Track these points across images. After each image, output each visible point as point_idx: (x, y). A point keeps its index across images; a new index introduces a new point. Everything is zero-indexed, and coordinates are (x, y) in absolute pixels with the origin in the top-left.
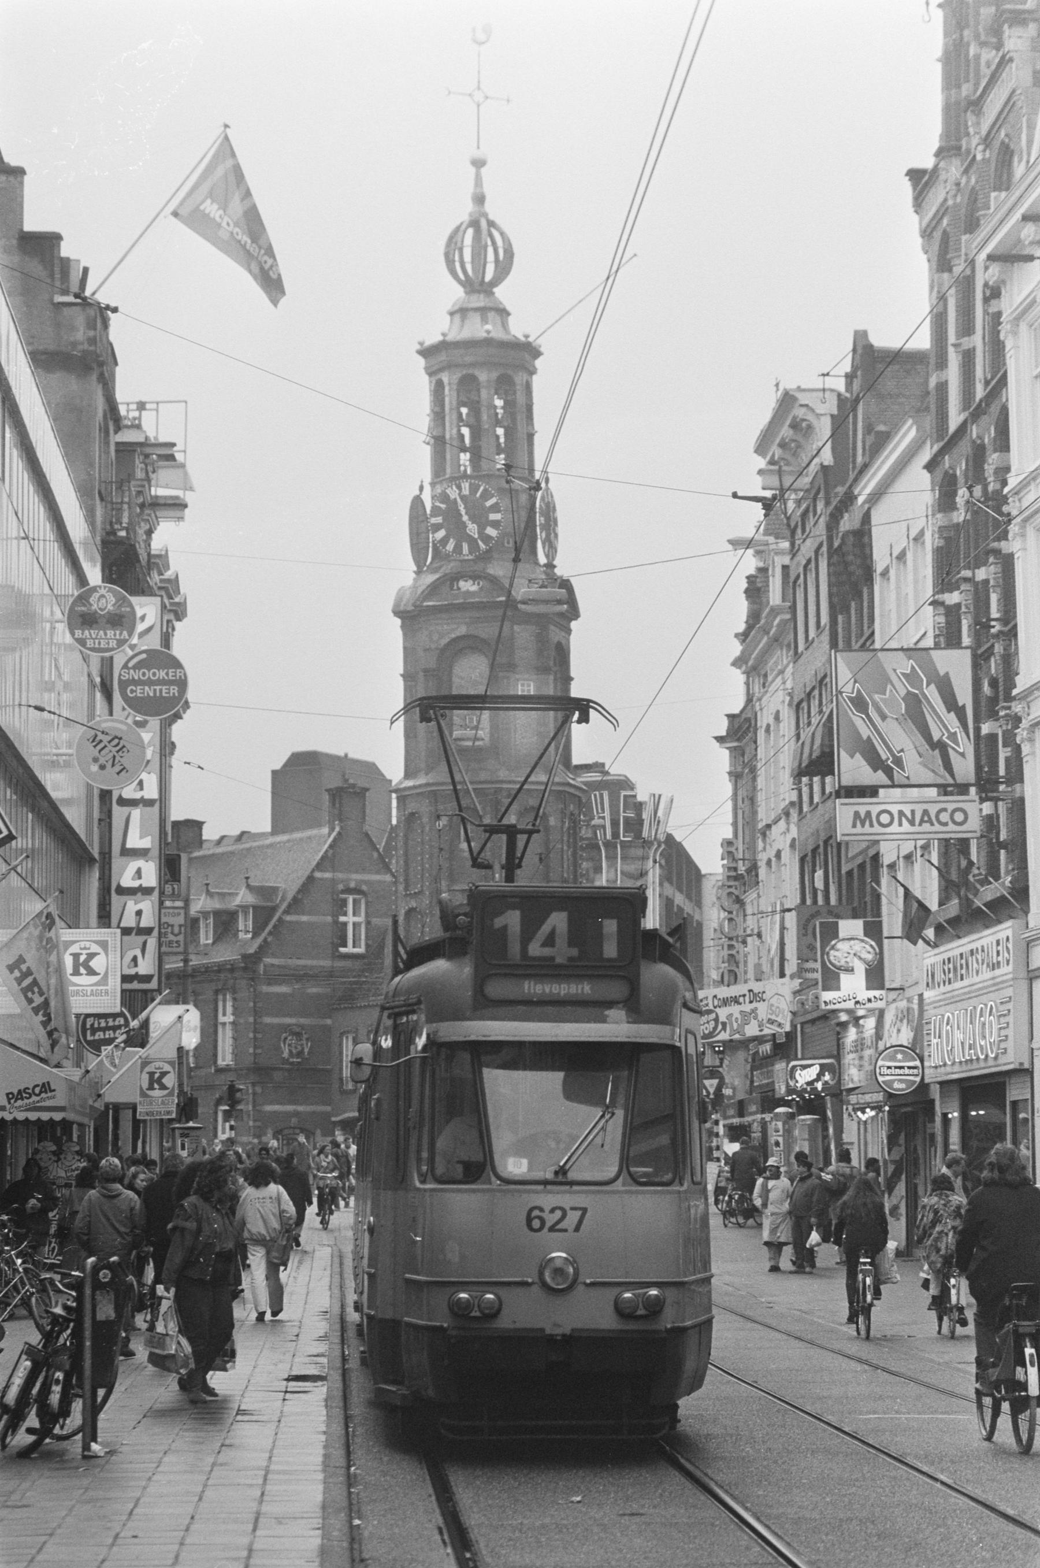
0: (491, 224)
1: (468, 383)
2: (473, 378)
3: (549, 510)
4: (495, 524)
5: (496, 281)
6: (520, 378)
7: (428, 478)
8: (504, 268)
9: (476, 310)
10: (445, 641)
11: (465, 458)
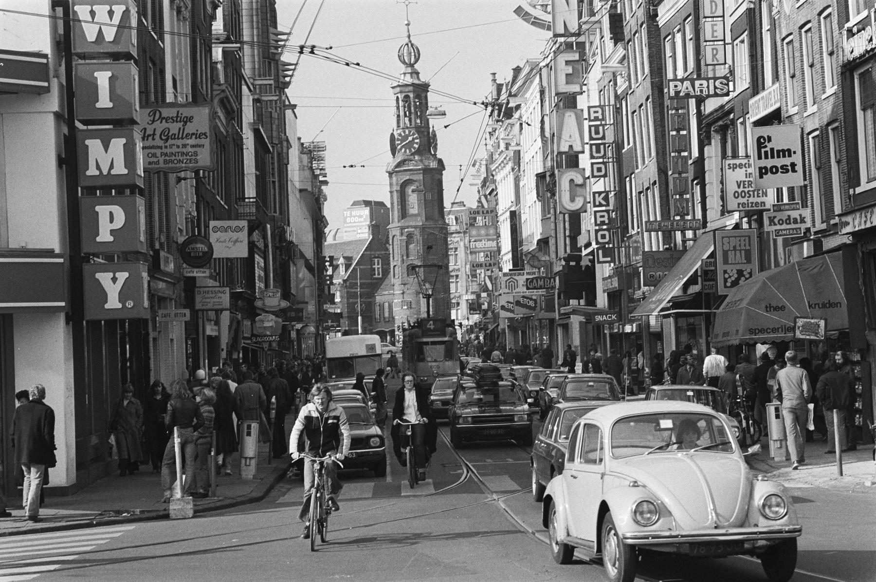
0: (412, 45)
5: (416, 62)
6: (423, 95)
7: (395, 128)
8: (417, 60)
11: (407, 119)
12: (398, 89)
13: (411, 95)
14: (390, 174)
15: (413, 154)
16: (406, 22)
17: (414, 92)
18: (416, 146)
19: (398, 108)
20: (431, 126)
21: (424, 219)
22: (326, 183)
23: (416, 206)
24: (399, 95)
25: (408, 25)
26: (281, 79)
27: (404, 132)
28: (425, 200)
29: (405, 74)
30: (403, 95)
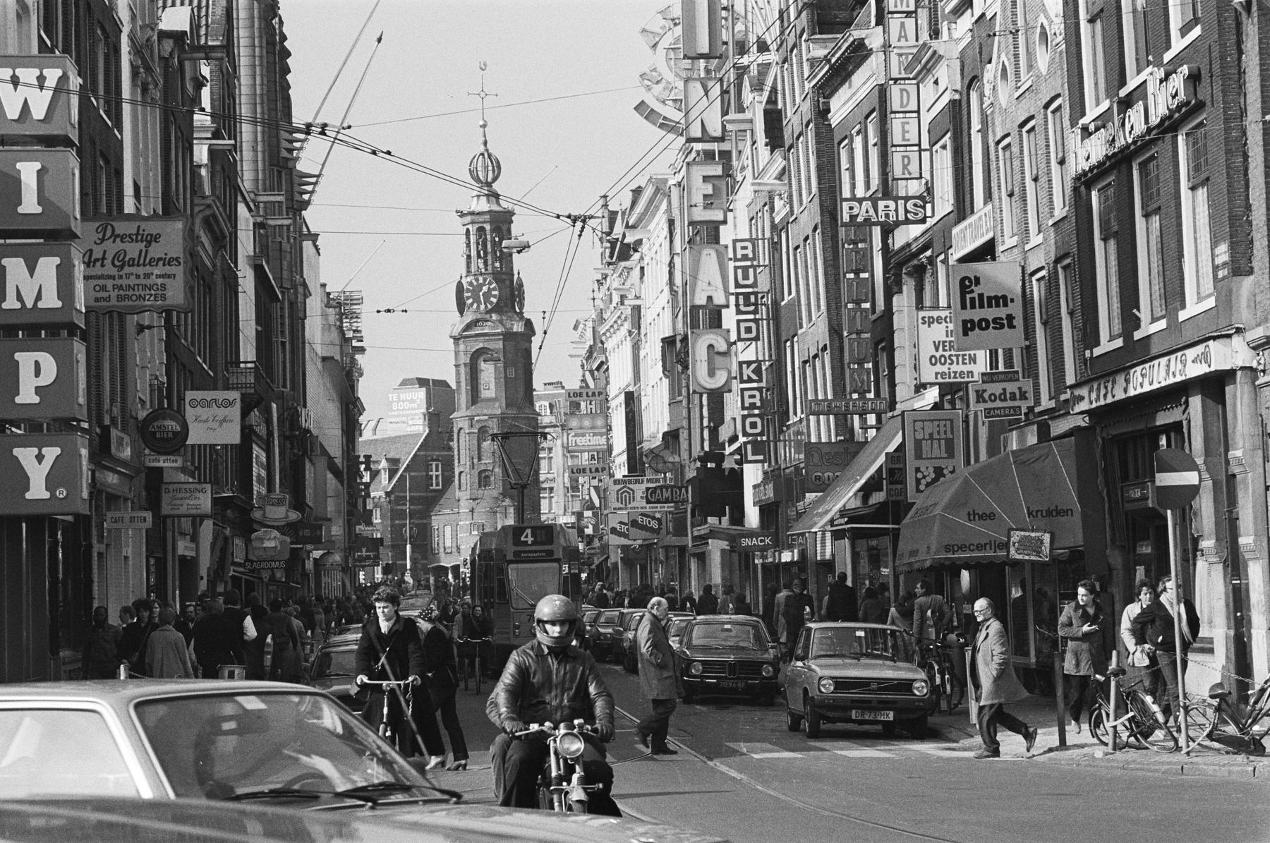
0: (490, 156)
1: (481, 230)
4: (495, 296)
5: (495, 179)
6: (504, 228)
12: (469, 219)
13: (488, 227)
14: (456, 339)
16: (481, 123)
17: (491, 222)
18: (494, 300)
19: (468, 245)
20: (515, 272)
22: (362, 350)
24: (470, 227)
25: (484, 126)
26: (297, 197)
27: (477, 280)
28: (506, 377)
30: (477, 226)
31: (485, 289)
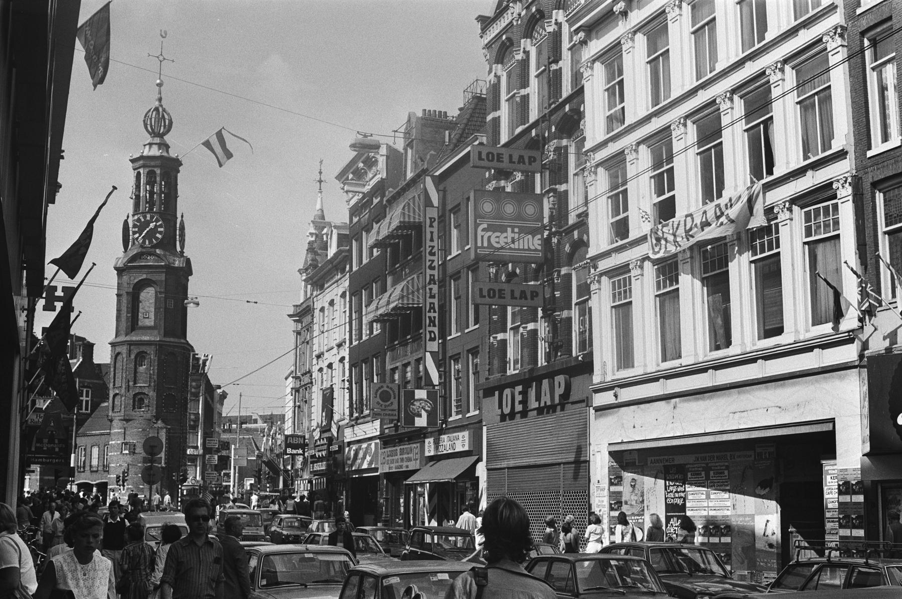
0: (164, 110)
1: (151, 175)
2: (154, 172)
3: (182, 228)
4: (160, 233)
7: (131, 213)
9: (156, 144)
10: (136, 281)
13: (158, 171)
14: (120, 271)
15: (155, 247)
16: (158, 81)
20: (179, 215)
21: (162, 332)
23: (152, 316)
24: (141, 170)
25: (160, 85)
27: (145, 217)
28: (166, 308)
29: (150, 144)
30: (147, 170)
31: (152, 225)
